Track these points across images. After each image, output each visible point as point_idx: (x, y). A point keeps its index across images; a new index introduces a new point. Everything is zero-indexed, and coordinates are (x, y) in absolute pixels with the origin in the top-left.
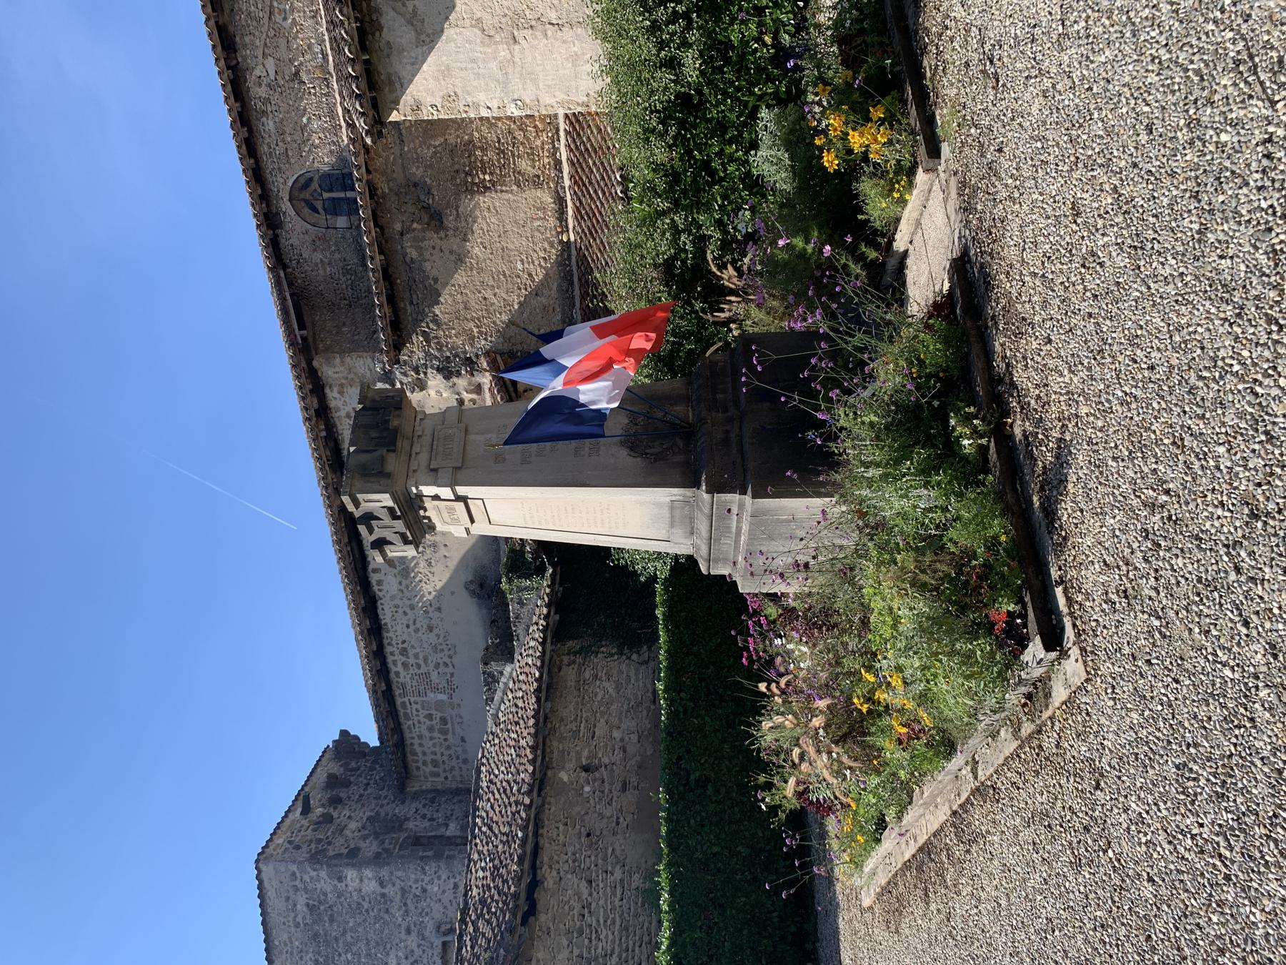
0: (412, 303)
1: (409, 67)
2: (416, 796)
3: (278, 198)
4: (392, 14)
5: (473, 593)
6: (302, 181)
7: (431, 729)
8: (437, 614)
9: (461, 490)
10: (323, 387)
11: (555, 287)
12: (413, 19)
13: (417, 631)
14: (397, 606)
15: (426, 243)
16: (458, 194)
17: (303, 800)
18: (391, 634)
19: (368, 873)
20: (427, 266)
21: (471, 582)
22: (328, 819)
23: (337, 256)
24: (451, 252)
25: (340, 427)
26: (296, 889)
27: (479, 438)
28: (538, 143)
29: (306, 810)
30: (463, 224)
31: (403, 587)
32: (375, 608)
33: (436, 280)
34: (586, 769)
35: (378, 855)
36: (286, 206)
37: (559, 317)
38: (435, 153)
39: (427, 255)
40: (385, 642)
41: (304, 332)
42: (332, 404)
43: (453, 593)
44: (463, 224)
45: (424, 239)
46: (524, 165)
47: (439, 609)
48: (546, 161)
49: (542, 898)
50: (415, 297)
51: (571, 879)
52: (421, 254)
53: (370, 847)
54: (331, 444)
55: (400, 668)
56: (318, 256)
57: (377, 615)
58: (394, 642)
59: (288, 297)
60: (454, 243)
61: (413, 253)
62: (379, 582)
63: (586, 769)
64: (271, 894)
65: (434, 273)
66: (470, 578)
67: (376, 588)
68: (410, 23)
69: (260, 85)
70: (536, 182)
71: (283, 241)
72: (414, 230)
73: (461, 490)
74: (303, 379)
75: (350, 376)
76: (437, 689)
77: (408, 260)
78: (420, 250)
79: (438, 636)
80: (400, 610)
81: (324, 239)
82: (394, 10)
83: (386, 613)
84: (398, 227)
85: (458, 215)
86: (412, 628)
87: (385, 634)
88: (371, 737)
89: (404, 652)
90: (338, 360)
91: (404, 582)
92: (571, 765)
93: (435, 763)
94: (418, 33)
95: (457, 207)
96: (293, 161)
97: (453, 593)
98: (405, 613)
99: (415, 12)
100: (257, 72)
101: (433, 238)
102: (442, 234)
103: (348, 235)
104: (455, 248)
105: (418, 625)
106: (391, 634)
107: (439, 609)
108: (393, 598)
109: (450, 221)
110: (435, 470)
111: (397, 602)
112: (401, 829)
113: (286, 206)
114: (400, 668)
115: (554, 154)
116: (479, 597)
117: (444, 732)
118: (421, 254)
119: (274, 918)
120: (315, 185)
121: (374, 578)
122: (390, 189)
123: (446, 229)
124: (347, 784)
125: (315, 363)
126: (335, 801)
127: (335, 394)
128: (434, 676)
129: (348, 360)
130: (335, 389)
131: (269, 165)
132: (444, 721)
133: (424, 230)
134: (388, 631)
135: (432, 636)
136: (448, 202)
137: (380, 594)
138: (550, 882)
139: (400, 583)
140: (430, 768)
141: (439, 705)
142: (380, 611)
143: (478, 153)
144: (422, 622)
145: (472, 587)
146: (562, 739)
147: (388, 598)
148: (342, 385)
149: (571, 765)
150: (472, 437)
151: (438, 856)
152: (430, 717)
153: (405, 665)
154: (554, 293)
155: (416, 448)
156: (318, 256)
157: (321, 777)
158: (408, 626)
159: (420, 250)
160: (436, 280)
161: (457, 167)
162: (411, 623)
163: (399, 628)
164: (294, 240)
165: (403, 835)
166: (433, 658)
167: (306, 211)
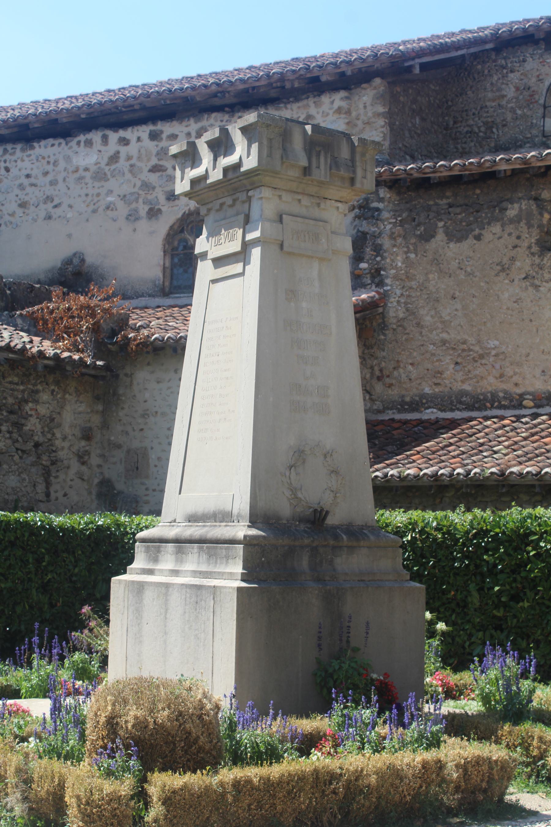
0: (450, 206)
5: (68, 262)
8: (43, 214)
9: (256, 253)
10: (346, 88)
11: (467, 387)
13: (21, 187)
14: (55, 163)
18: (19, 154)
20: (496, 228)
21: (83, 261)
23: (509, 116)
24: (513, 259)
25: (295, 106)
27: (315, 273)
31: (81, 172)
32: (55, 136)
33: (478, 238)
37: (427, 390)
39: (510, 228)
40: (9, 147)
41: (417, 70)
42: (325, 99)
43: (69, 236)
45: (530, 226)
47: (49, 217)
50: (458, 210)
52: (511, 221)
54: (273, 94)
56: (510, 92)
57: (45, 137)
58: (7, 157)
59: (460, 53)
60: (524, 263)
61: (512, 212)
62: (89, 143)
65: (487, 235)
66: (89, 260)
67: (82, 138)
71: (530, 50)
72: (541, 215)
73: (256, 253)
74: (358, 65)
75: (359, 123)
77: (504, 204)
78: (516, 221)
79: (12, 215)
80: (50, 168)
81: (530, 102)
83: (47, 149)
84: (545, 195)
86: (26, 182)
87: (19, 146)
90: (381, 109)
91: (88, 175)
97: (69, 236)
98: (46, 174)
101: (530, 237)
102: (535, 249)
103: (534, 132)
104: (518, 264)
105: (29, 190)
106: (19, 154)
107: (49, 217)
108: (68, 159)
110: (281, 220)
111: (62, 164)
116: (62, 271)
118: (511, 221)
121: (96, 136)
123: (541, 254)
125: (377, 81)
127: (338, 103)
129: (381, 122)
130: (344, 104)
133: (540, 226)
134: (23, 150)
135: (13, 207)
137: (73, 143)
139: (86, 169)
142: (51, 141)
145: (76, 261)
147: (70, 153)
148: (348, 112)
150: (316, 265)
154: (458, 386)
155: (306, 201)
156: (510, 92)
158: (28, 176)
159: (516, 221)
160: (478, 238)
162: (32, 180)
163: (27, 164)
164: (531, 64)
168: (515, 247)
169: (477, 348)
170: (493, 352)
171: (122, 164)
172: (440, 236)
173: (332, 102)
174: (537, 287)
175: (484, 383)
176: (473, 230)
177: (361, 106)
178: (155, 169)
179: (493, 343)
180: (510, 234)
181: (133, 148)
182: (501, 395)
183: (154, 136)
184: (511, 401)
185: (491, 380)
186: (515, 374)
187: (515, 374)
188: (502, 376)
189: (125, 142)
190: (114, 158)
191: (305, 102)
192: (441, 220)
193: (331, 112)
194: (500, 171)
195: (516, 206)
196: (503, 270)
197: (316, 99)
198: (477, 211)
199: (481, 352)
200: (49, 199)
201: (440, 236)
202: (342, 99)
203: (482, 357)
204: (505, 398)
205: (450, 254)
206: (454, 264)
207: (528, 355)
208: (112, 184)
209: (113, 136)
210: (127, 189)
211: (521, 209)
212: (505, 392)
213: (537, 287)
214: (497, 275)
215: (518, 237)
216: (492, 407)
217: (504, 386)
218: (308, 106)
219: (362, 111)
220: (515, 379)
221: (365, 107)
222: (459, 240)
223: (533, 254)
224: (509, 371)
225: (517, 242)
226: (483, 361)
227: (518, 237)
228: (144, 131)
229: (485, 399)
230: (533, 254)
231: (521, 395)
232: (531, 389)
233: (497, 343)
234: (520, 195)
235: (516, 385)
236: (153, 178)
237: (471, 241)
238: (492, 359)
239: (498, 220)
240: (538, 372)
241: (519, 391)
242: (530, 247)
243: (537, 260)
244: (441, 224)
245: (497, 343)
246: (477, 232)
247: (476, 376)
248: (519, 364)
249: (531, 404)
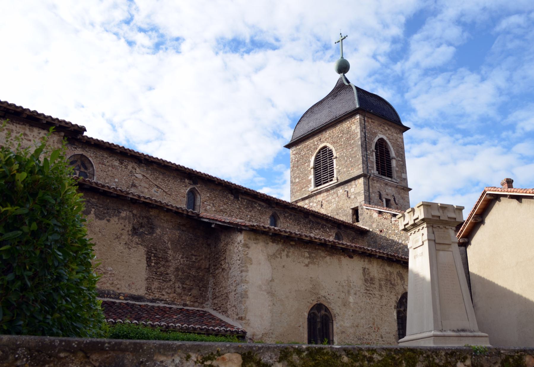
1: (261, 248)
3: (83, 148)
4: (277, 248)
6: (88, 165)
12: (274, 256)
15: (128, 223)
16: (147, 247)
20: (116, 219)
24: (121, 234)
25: (18, 126)
28: (164, 293)
30: (134, 245)
33: (108, 221)
36: (79, 151)
38: (165, 242)
39: (121, 221)
42: (36, 130)
44: (134, 245)
45: (129, 223)
46: (156, 284)
48: (157, 296)
50: (101, 206)
52: (122, 218)
60: (125, 237)
61: (123, 214)
68: (274, 254)
69: (133, 168)
70: (148, 289)
78: (124, 218)
82: (278, 250)
85: (138, 244)
94: (271, 256)
95: (142, 245)
96: (100, 165)
99: (277, 257)
100: (138, 169)
101: (129, 228)
102: (130, 233)
104: (123, 237)
109: (136, 239)
113: (79, 151)
115: (159, 300)
118: (122, 218)
120: (82, 169)
122: (151, 215)
123: (133, 236)
131: (100, 153)
136: (144, 242)
143: (163, 263)
159: (124, 218)
160: (108, 221)
161: (158, 251)
167: (72, 159)
168: (123, 229)
169: (103, 269)
170: (110, 272)
172: (92, 216)
173: (40, 133)
174: (130, 249)
175: (105, 286)
176: (106, 217)
177: (52, 141)
179: (110, 268)
180: (121, 224)
182: (112, 292)
184: (115, 295)
185: (108, 285)
186: (118, 284)
187: (118, 284)
188: (113, 283)
191: (24, 126)
192: (94, 208)
193: (38, 137)
194: (129, 197)
195: (125, 213)
196: (117, 238)
197: (31, 128)
198: (108, 209)
199: (104, 271)
201: (92, 216)
202: (45, 134)
203: (104, 273)
204: (113, 294)
205: (96, 224)
206: (97, 229)
207: (123, 277)
211: (126, 215)
212: (113, 291)
213: (130, 249)
214: (115, 239)
215: (125, 226)
216: (107, 297)
217: (112, 288)
218: (26, 130)
219: (51, 143)
220: (118, 286)
221: (54, 143)
222: (100, 219)
223: (129, 235)
224: (115, 282)
225: (124, 227)
226: (105, 276)
227: (125, 226)
229: (105, 293)
230: (129, 235)
231: (120, 294)
232: (124, 292)
233: (112, 269)
234: (126, 208)
235: (118, 289)
237: (105, 221)
238: (109, 275)
239: (116, 216)
240: (127, 285)
241: (119, 292)
242: (128, 231)
243: (131, 238)
244: (93, 210)
245: (112, 269)
246: (108, 218)
247: (101, 282)
248: (120, 280)
249: (123, 298)
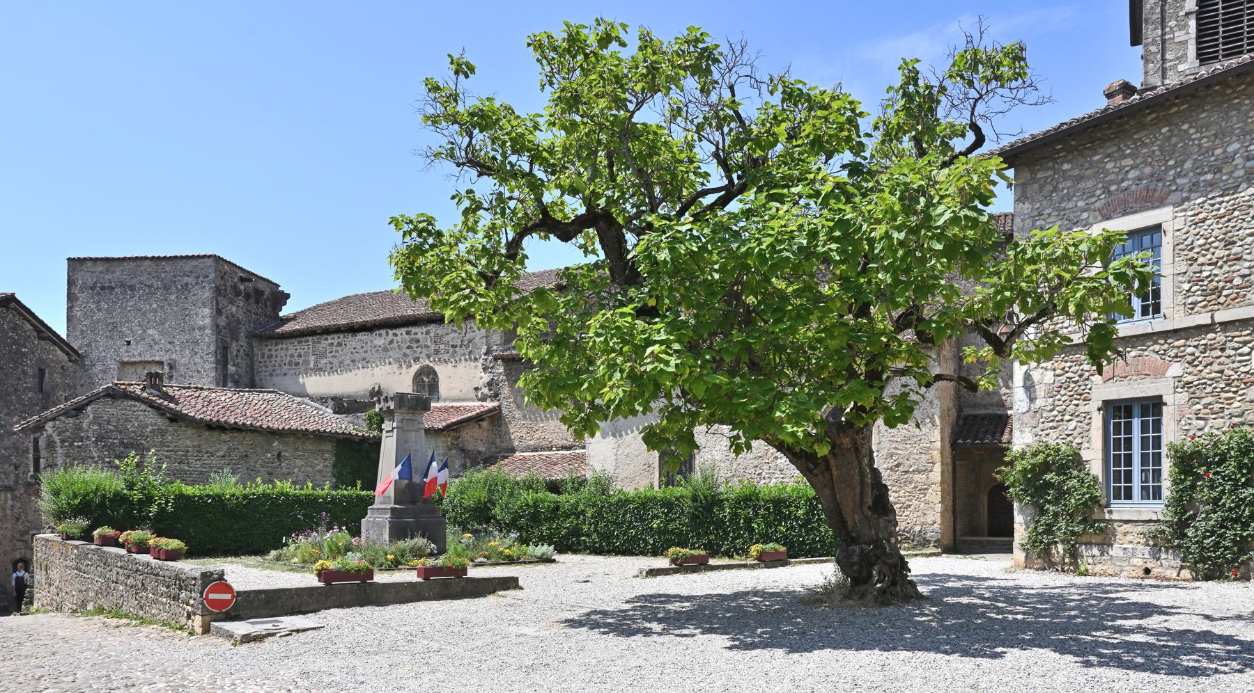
2: (250, 345)
7: (292, 356)
17: (248, 277)
19: (208, 320)
22: (238, 293)
26: (198, 278)
29: (242, 280)
34: (279, 455)
35: (217, 326)
49: (216, 434)
51: (225, 448)
53: (222, 321)
55: (330, 341)
62: (380, 335)
63: (279, 455)
64: (195, 263)
76: (316, 362)
83: (362, 336)
88: (285, 312)
89: (340, 344)
92: (281, 447)
93: (270, 356)
112: (232, 339)
114: (330, 341)
117: (290, 363)
119: (180, 263)
121: (383, 332)
124: (257, 302)
126: (247, 296)
128: (324, 361)
132: (297, 364)
135: (349, 362)
138: (224, 437)
140: (267, 353)
141: (307, 362)
144: (357, 357)
146: (294, 443)
149: (281, 447)
151: (217, 362)
152: (300, 356)
153: (332, 344)
157: (261, 286)
165: (228, 340)
166: (336, 361)
171: (395, 345)
178: (409, 347)
181: (399, 338)
183: (408, 333)
189: (395, 335)
190: (391, 342)
200: (364, 359)
208: (391, 353)
209: (391, 332)
210: (397, 356)
228: (404, 330)
236: (408, 351)
